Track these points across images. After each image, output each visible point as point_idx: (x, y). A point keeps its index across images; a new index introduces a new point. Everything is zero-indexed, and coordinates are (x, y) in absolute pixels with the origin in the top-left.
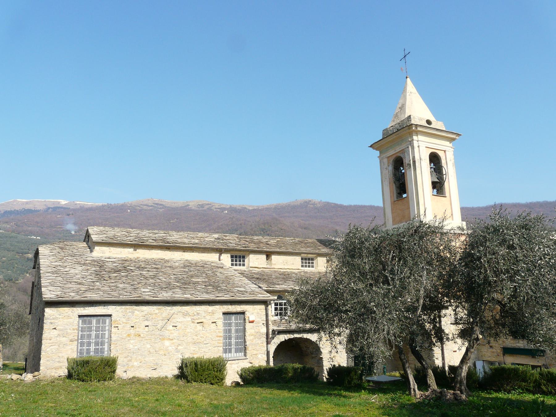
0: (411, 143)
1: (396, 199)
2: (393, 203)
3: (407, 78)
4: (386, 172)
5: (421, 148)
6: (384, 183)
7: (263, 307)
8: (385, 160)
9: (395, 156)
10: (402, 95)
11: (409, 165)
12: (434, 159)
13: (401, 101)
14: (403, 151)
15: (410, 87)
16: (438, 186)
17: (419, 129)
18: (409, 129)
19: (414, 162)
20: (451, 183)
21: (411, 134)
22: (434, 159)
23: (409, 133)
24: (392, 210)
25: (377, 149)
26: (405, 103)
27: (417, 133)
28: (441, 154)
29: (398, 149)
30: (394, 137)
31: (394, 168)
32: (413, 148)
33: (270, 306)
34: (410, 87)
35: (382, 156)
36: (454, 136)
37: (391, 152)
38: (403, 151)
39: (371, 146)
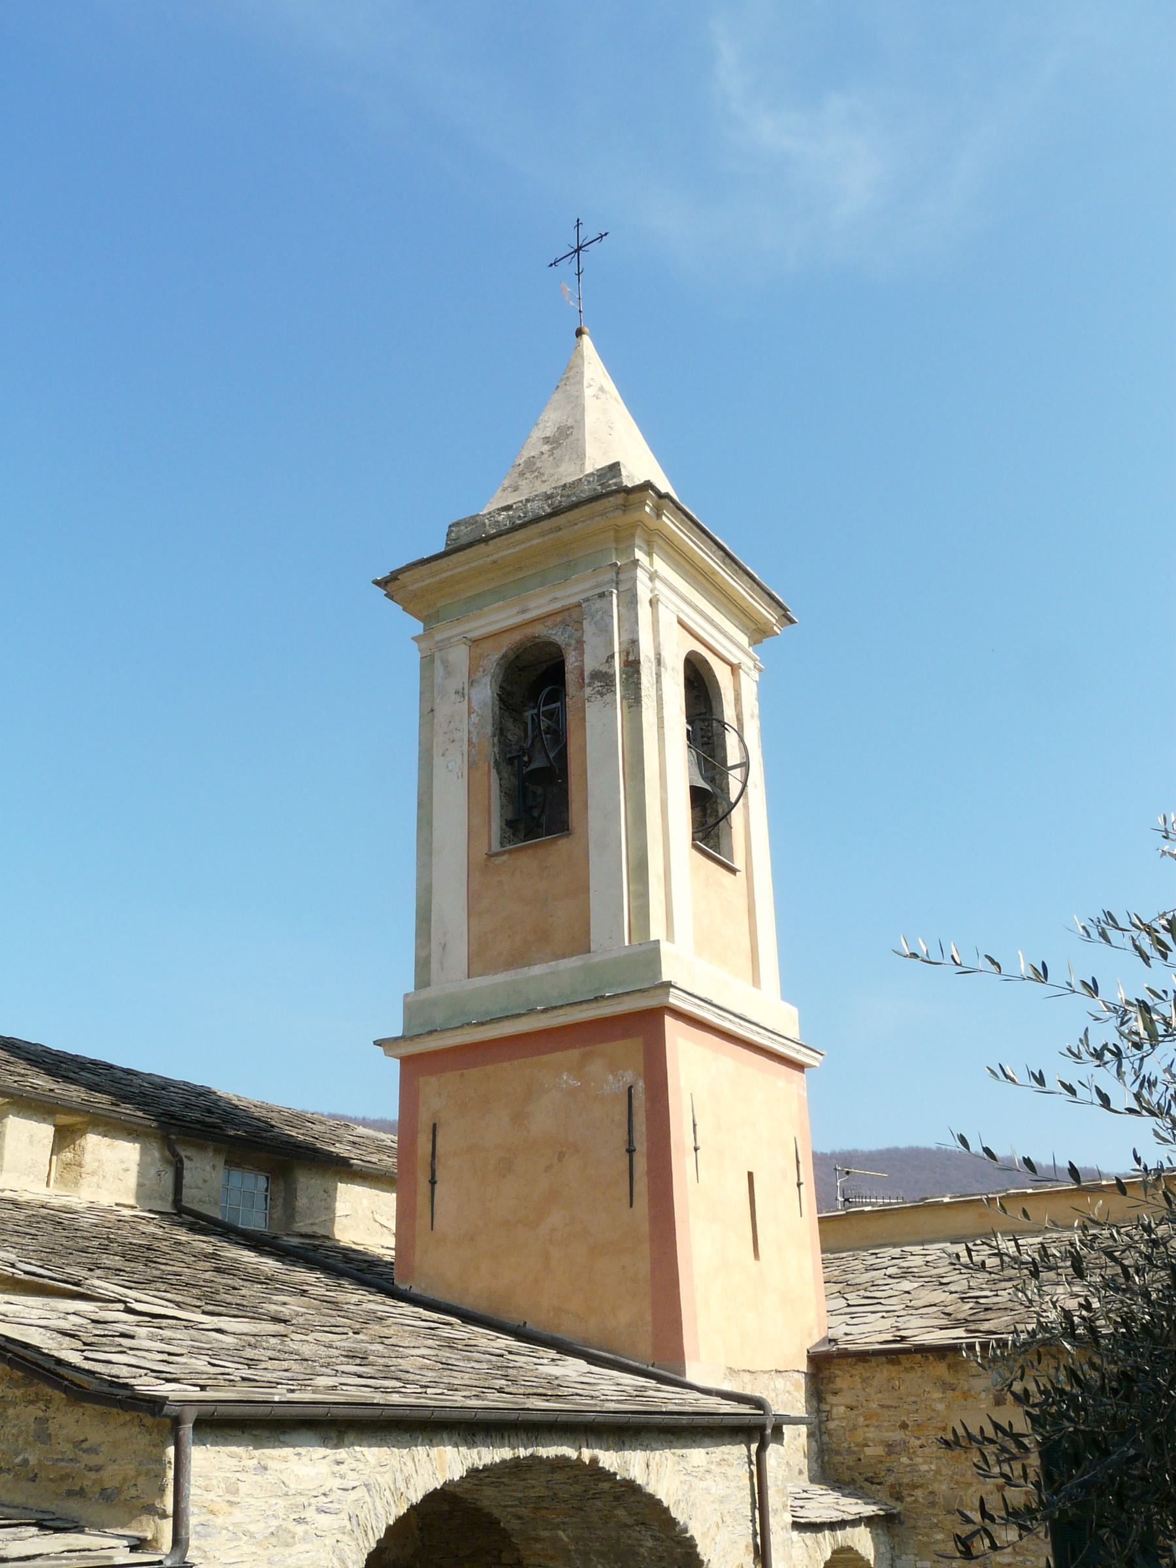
0: (622, 578)
1: (496, 847)
2: (482, 868)
3: (579, 333)
4: (451, 709)
5: (667, 616)
6: (438, 761)
7: (736, 1454)
8: (459, 655)
9: (517, 637)
10: (558, 396)
11: (604, 679)
12: (700, 685)
13: (550, 421)
14: (572, 616)
15: (594, 369)
16: (710, 812)
17: (669, 522)
18: (625, 507)
19: (632, 666)
20: (751, 821)
21: (623, 539)
22: (700, 685)
23: (617, 530)
24: (473, 897)
25: (409, 605)
26: (580, 423)
27: (656, 540)
28: (722, 673)
29: (541, 603)
30: (532, 539)
31: (501, 698)
32: (630, 601)
33: (772, 1450)
34: (594, 369)
35: (438, 637)
36: (769, 615)
37: (503, 619)
38: (572, 616)
39: (377, 583)
